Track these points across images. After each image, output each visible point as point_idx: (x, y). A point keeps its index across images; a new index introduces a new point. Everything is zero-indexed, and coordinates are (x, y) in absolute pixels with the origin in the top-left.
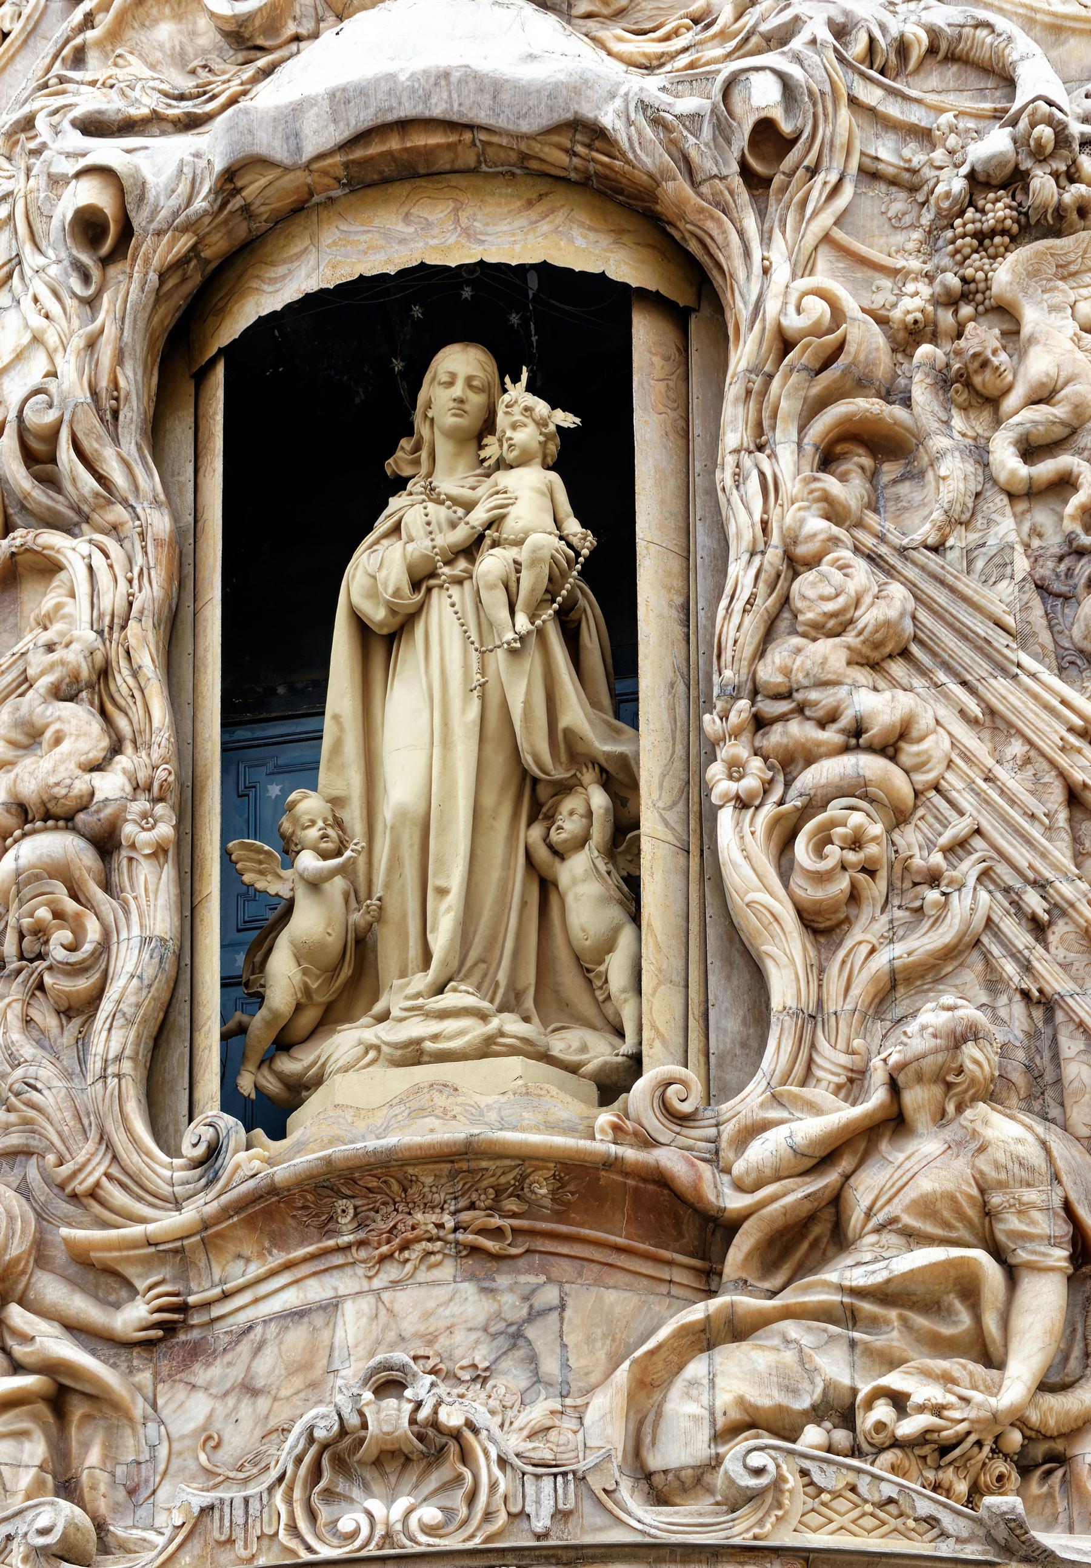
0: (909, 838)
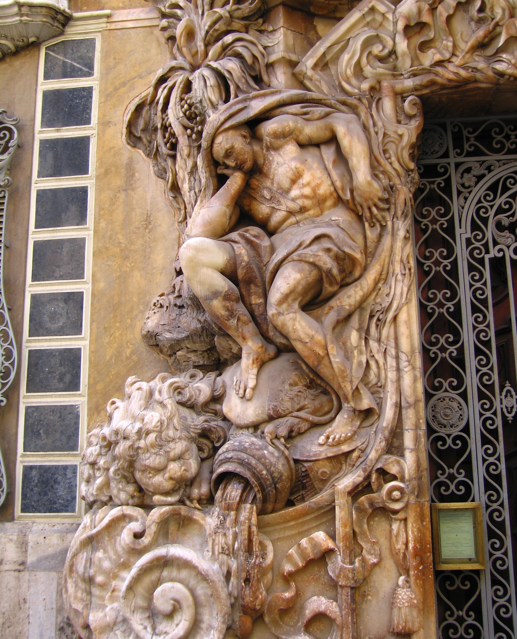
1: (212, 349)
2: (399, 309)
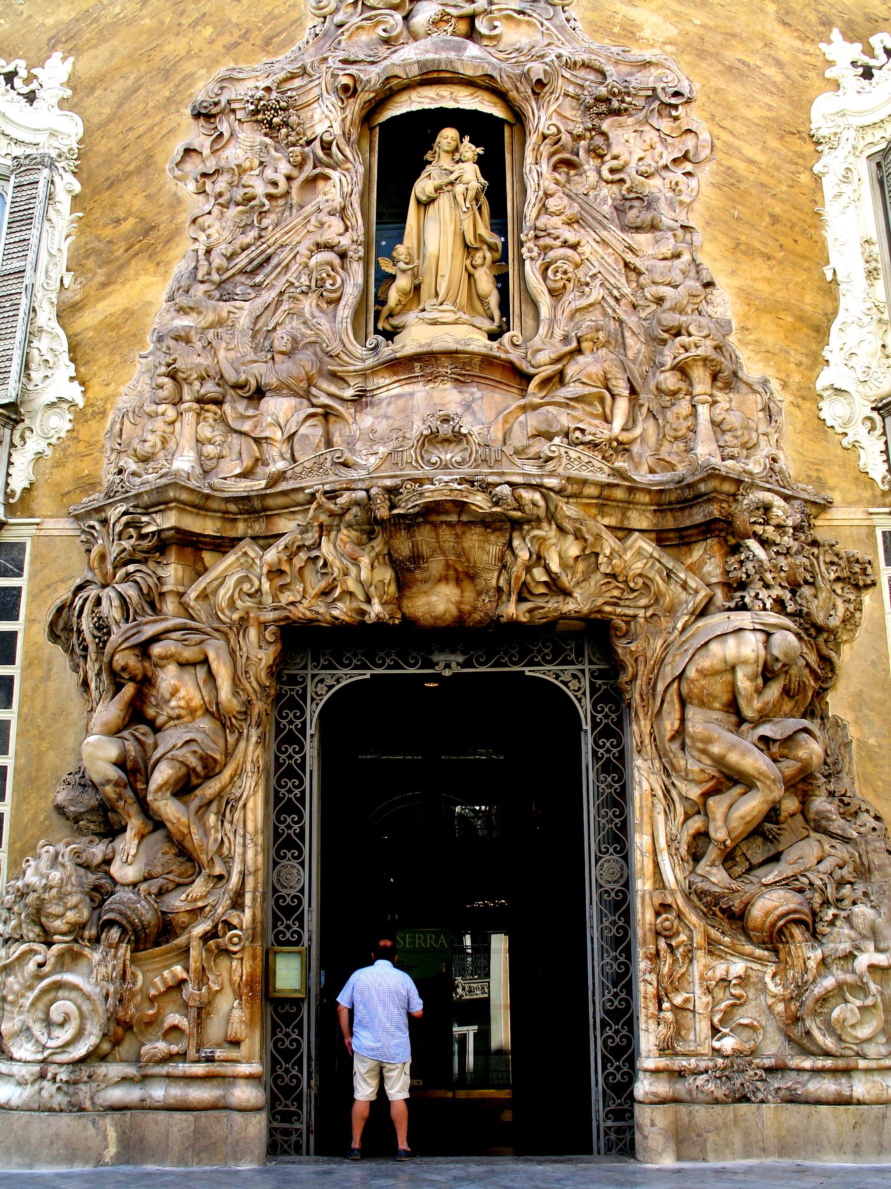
0: (580, 273)
2: (247, 799)
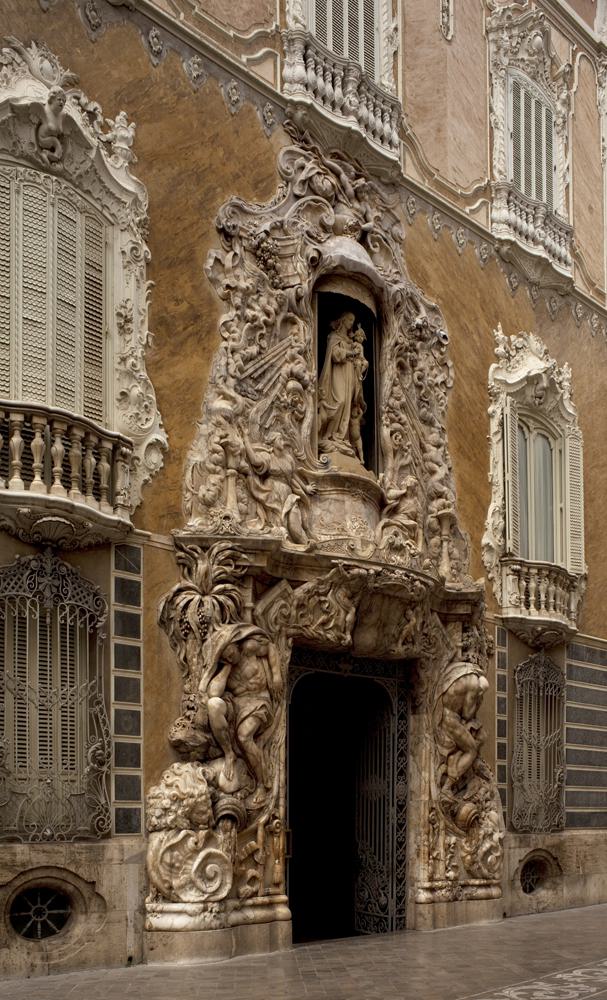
1: (207, 751)
